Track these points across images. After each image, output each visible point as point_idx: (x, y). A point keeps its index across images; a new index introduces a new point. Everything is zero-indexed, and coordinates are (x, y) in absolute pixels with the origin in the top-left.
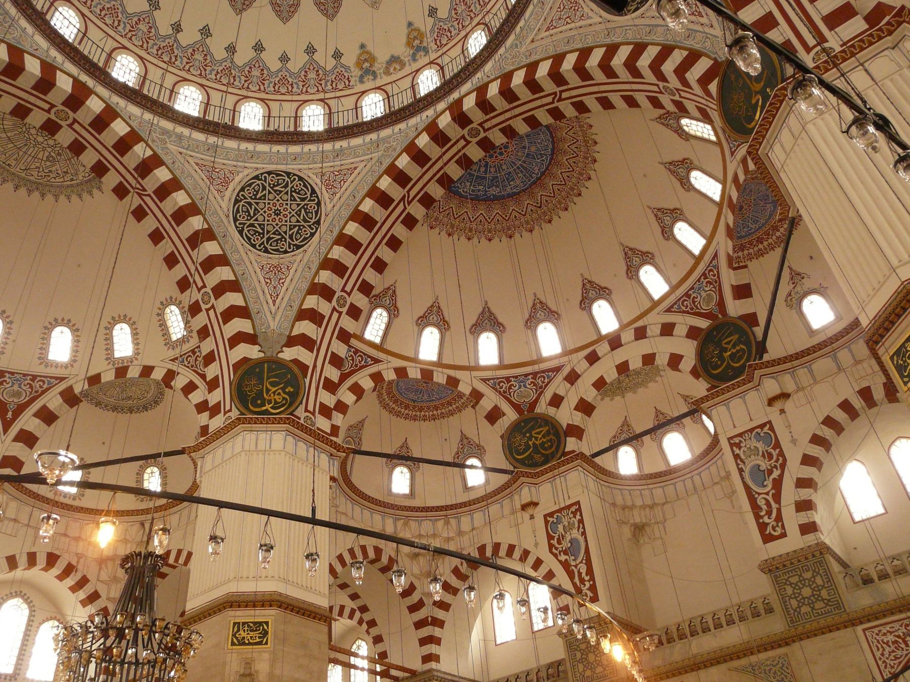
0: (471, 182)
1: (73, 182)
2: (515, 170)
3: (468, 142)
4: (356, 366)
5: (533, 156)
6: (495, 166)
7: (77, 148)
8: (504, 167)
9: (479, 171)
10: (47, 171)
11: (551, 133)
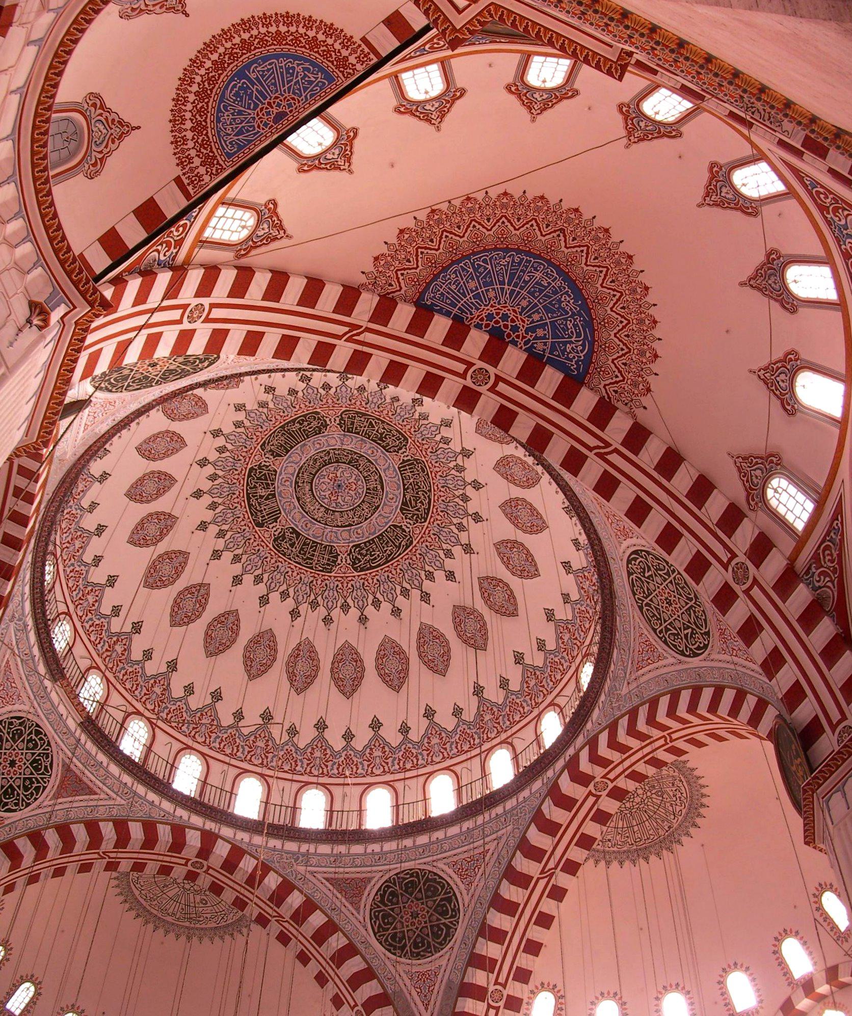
0: (565, 343)
1: (683, 780)
2: (522, 288)
3: (498, 379)
4: (834, 572)
5: (485, 277)
6: (529, 316)
7: (637, 777)
8: (524, 303)
9: (544, 337)
10: (675, 799)
11: (428, 285)
